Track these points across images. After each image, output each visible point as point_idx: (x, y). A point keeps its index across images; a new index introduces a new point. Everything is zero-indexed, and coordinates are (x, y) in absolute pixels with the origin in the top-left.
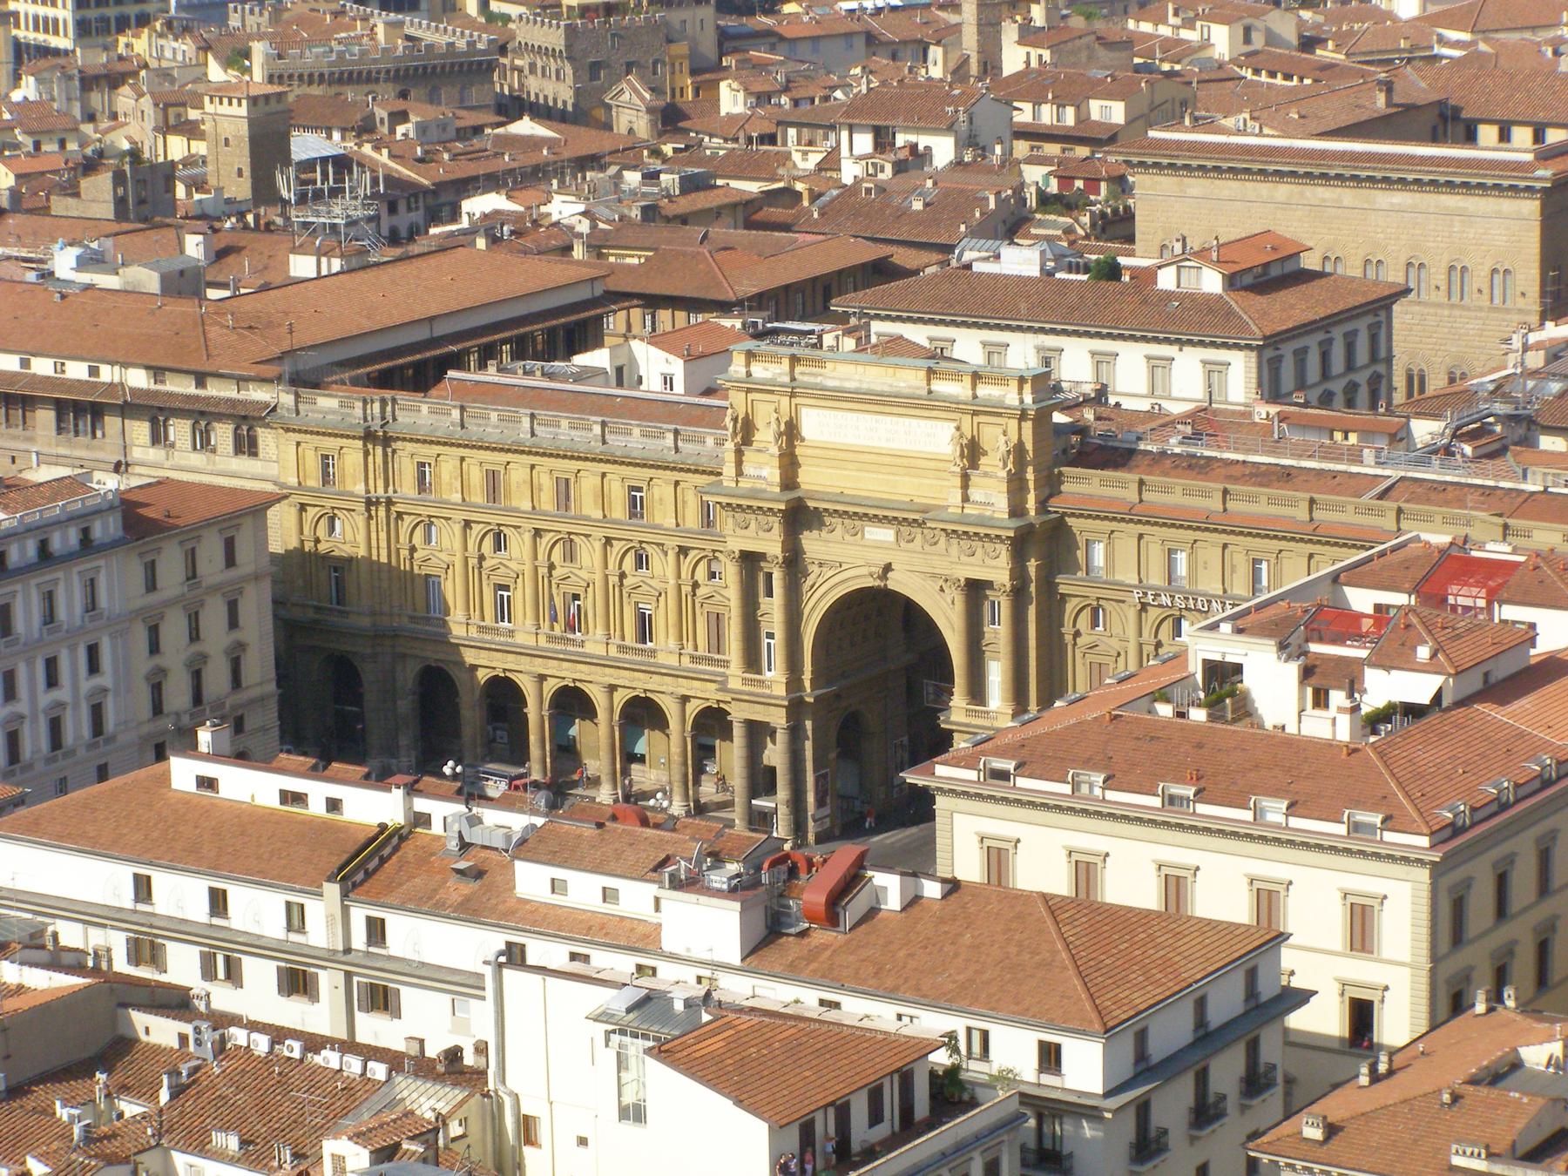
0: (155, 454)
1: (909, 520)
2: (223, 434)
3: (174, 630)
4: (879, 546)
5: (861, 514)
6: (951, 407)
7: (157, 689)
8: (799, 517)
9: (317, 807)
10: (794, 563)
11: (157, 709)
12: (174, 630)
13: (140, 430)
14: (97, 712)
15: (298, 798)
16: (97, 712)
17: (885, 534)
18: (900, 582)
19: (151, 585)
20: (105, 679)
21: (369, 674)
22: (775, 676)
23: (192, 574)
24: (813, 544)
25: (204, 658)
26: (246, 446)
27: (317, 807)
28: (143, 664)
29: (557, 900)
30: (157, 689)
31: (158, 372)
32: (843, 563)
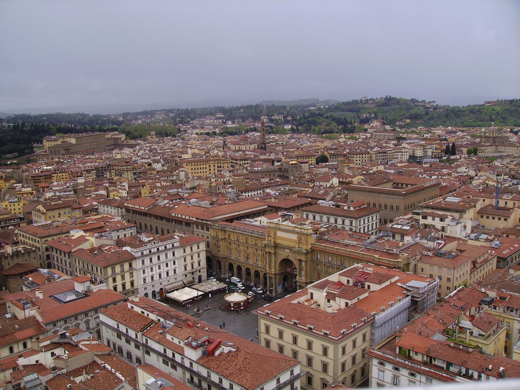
0: (197, 230)
1: (291, 249)
2: (205, 229)
3: (189, 259)
4: (287, 252)
5: (284, 248)
6: (297, 233)
7: (185, 267)
8: (276, 246)
9: (146, 315)
10: (275, 254)
11: (186, 269)
12: (189, 259)
13: (195, 227)
14: (175, 270)
15: (143, 313)
16: (175, 270)
17: (288, 251)
18: (290, 258)
19: (184, 252)
20: (176, 266)
21: (222, 263)
22: (273, 270)
23: (191, 250)
24: (279, 251)
25: (194, 262)
26: (208, 230)
27: (146, 315)
28: (183, 263)
29: (172, 341)
30: (185, 267)
31: (197, 219)
32: (284, 254)
